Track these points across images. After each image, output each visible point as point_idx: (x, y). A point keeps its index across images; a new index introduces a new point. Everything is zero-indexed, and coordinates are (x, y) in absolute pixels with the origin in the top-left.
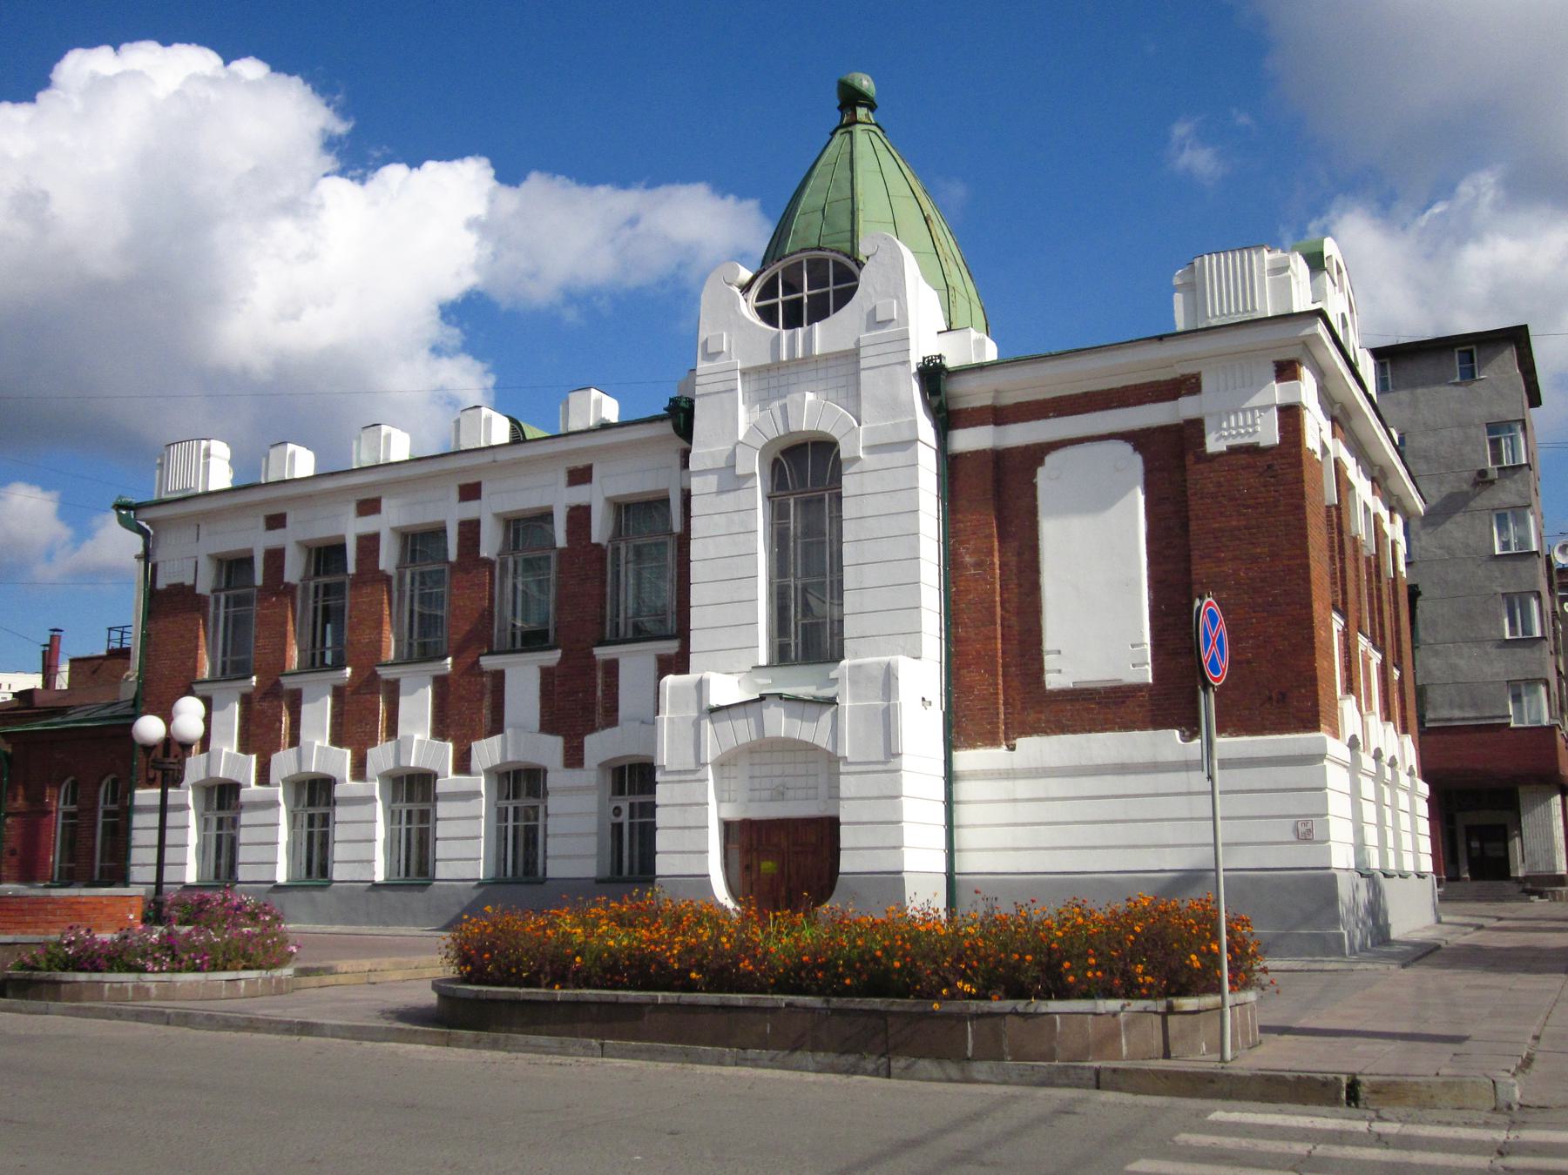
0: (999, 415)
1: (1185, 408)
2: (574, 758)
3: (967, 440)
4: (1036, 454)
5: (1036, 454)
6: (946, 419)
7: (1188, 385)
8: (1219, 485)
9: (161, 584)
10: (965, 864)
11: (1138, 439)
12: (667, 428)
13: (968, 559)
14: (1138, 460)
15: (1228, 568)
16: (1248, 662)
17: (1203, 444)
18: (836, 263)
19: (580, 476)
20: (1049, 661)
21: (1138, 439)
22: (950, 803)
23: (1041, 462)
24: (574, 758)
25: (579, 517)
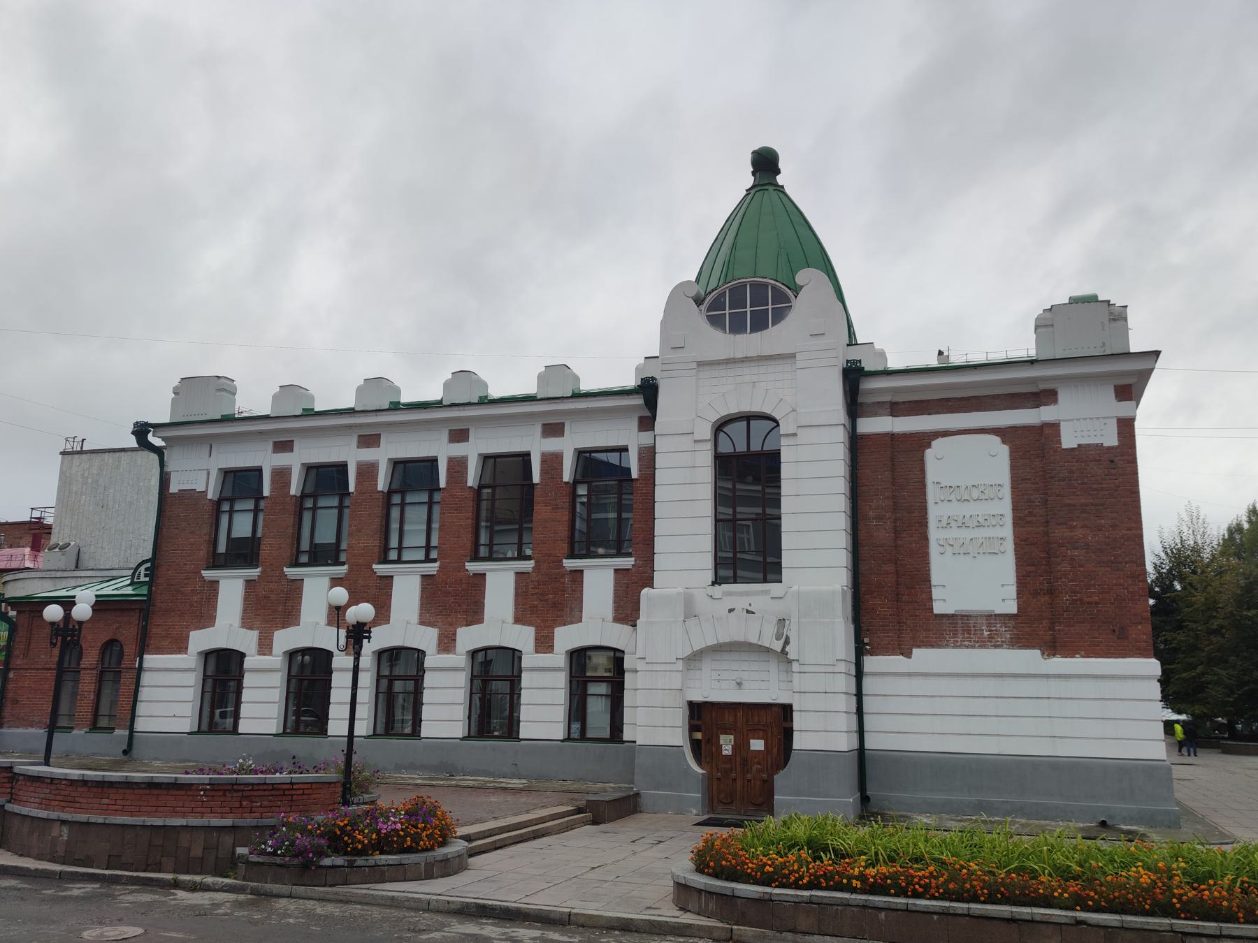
0: (896, 409)
1: (1045, 414)
2: (265, 646)
3: (870, 425)
4: (924, 440)
5: (924, 440)
6: (855, 406)
7: (1046, 396)
8: (1071, 472)
9: (174, 488)
10: (869, 745)
11: (1004, 433)
12: (638, 401)
13: (871, 513)
14: (1005, 449)
15: (1079, 533)
16: (1097, 603)
17: (1059, 442)
18: (773, 288)
19: (459, 436)
20: (936, 593)
21: (1004, 433)
22: (859, 695)
23: (929, 446)
24: (265, 646)
25: (457, 466)
